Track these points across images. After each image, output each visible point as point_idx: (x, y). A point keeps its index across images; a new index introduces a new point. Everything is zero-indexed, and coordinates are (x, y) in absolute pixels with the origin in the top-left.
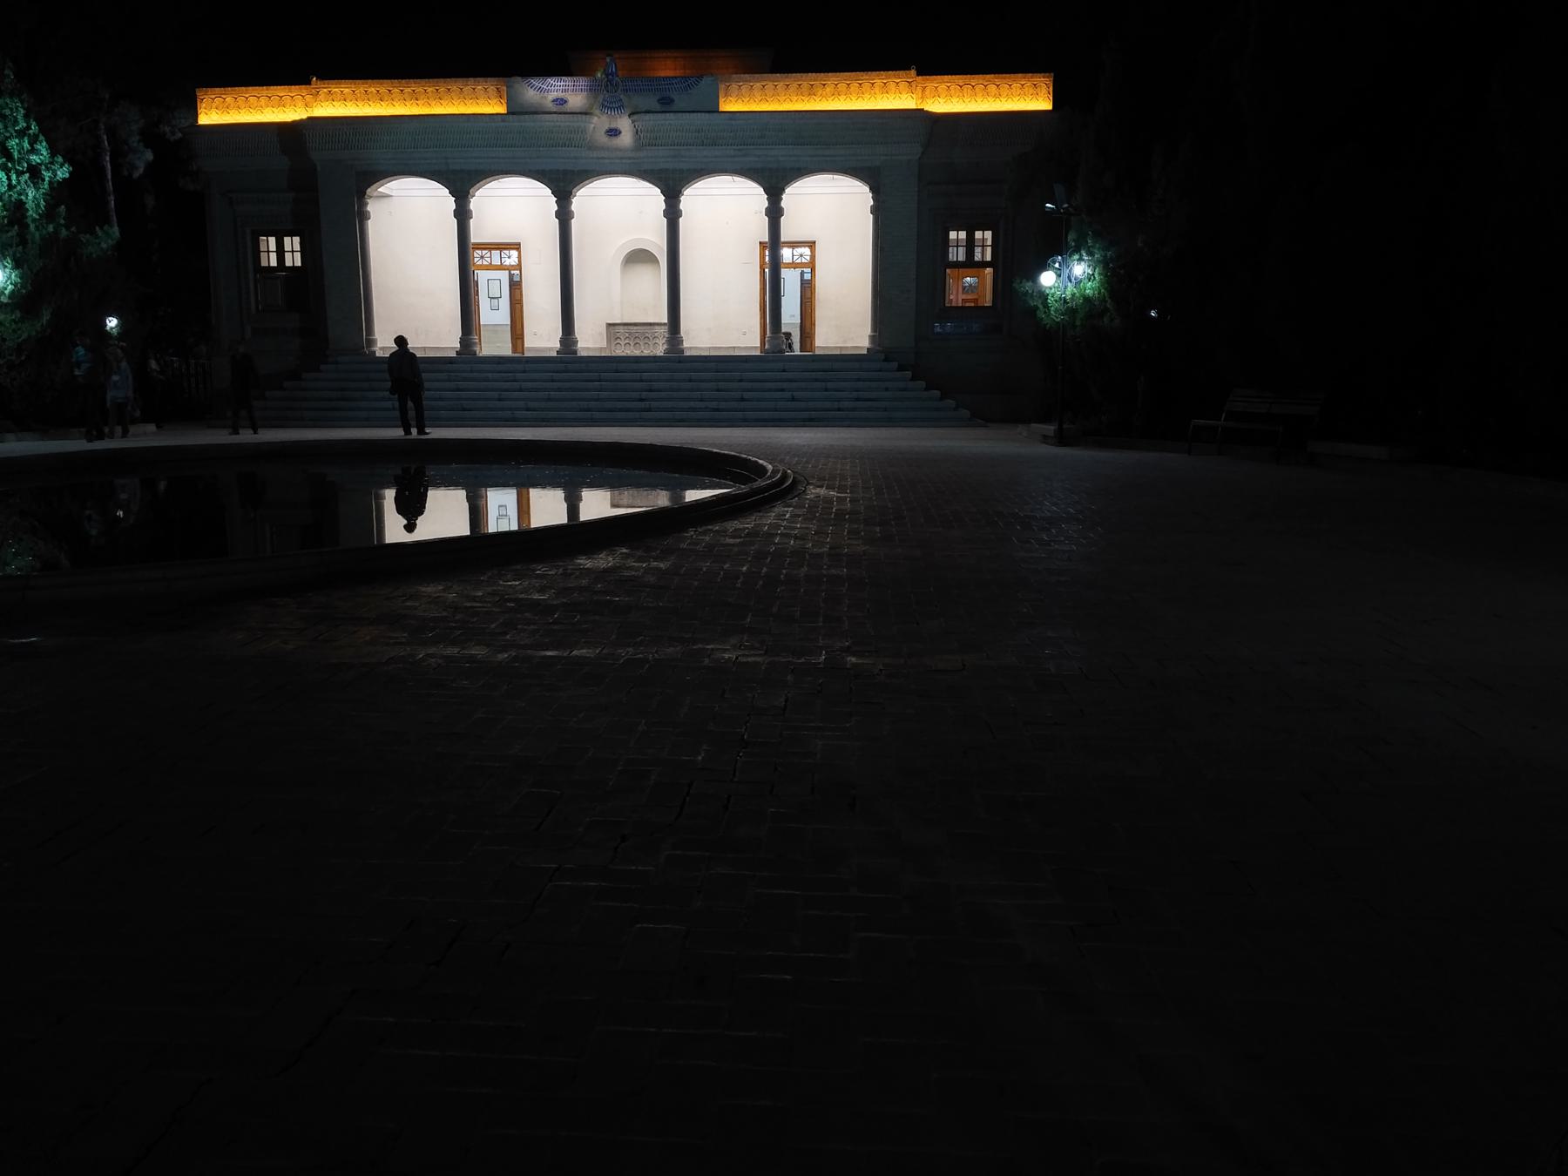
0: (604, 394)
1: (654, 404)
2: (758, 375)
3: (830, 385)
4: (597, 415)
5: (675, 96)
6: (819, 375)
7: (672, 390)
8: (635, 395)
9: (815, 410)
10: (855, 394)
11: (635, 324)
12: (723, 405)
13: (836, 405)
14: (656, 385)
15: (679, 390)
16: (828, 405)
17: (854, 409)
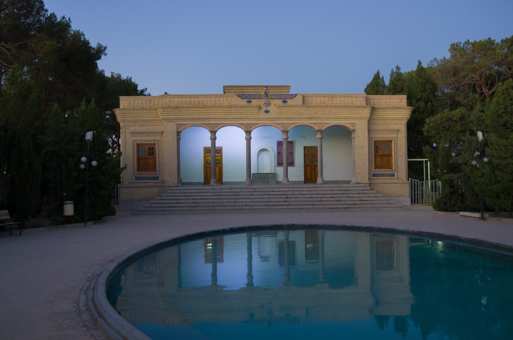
0: (272, 200)
1: (291, 203)
2: (324, 192)
3: (350, 195)
4: (272, 207)
5: (288, 100)
6: (345, 192)
7: (295, 198)
8: (283, 200)
9: (348, 204)
10: (359, 199)
12: (315, 203)
13: (354, 203)
14: (289, 196)
15: (297, 198)
16: (351, 203)
17: (361, 204)
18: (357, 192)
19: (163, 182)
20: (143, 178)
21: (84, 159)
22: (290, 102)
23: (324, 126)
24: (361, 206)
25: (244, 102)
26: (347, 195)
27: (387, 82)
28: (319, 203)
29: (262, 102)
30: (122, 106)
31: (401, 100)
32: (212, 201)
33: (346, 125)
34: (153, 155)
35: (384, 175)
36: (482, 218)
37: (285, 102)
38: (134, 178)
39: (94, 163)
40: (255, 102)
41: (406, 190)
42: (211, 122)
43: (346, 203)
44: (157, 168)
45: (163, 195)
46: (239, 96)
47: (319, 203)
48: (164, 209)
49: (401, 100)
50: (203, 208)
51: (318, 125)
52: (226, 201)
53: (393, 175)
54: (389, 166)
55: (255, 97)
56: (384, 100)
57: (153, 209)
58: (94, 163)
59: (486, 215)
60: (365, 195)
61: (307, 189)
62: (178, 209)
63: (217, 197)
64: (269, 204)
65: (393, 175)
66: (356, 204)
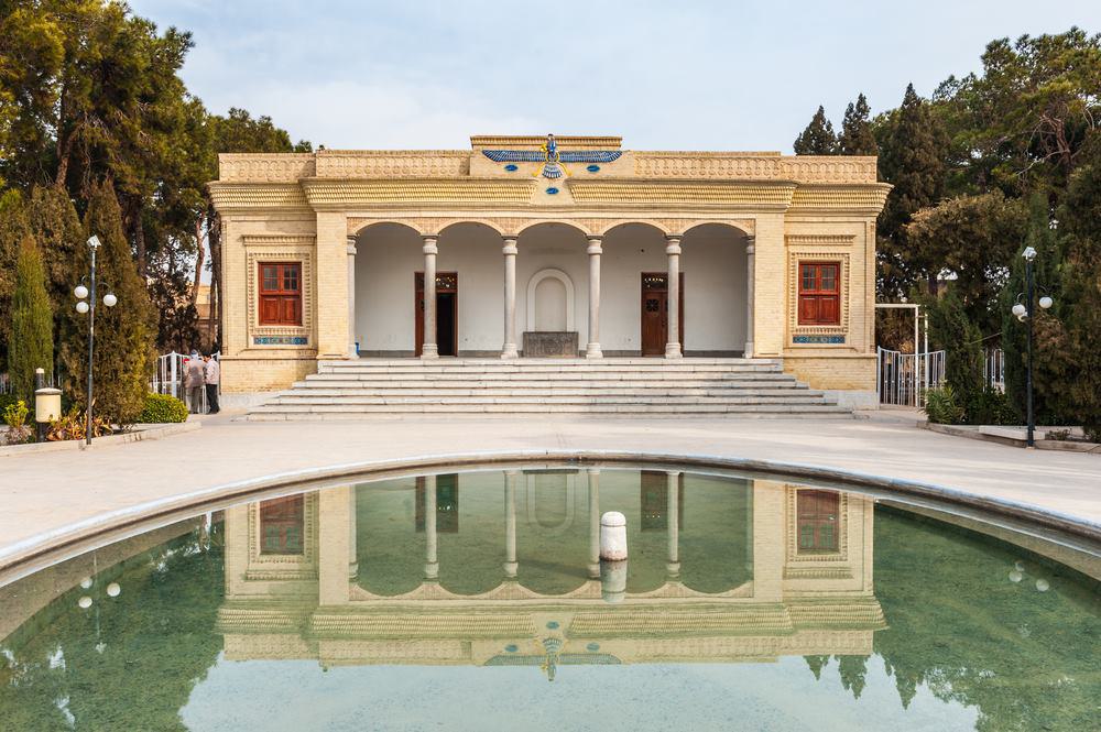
0: (555, 392)
4: (554, 409)
5: (599, 165)
8: (583, 392)
9: (729, 404)
10: (757, 392)
11: (546, 333)
12: (655, 400)
16: (738, 400)
18: (752, 377)
19: (316, 350)
20: (272, 340)
21: (81, 291)
22: (606, 170)
23: (682, 226)
24: (760, 408)
25: (499, 170)
26: (728, 384)
27: (838, 129)
28: (664, 400)
29: (540, 168)
30: (221, 179)
31: (862, 169)
32: (418, 392)
33: (733, 224)
34: (294, 286)
35: (819, 340)
36: (1030, 442)
37: (593, 169)
38: (251, 340)
39: (110, 300)
40: (524, 170)
41: (870, 373)
42: (424, 214)
43: (726, 400)
44: (304, 314)
45: (308, 377)
46: (487, 154)
47: (664, 400)
48: (307, 409)
49: (862, 169)
50: (396, 409)
51: (669, 222)
52: (451, 392)
53: (841, 339)
54: (835, 317)
55: (525, 157)
56: (823, 169)
57: (282, 409)
58: (110, 300)
59: (1040, 433)
60: (770, 384)
61: (637, 368)
62: (340, 409)
63: (431, 384)
64: (548, 400)
65: (841, 339)
66: (748, 404)
